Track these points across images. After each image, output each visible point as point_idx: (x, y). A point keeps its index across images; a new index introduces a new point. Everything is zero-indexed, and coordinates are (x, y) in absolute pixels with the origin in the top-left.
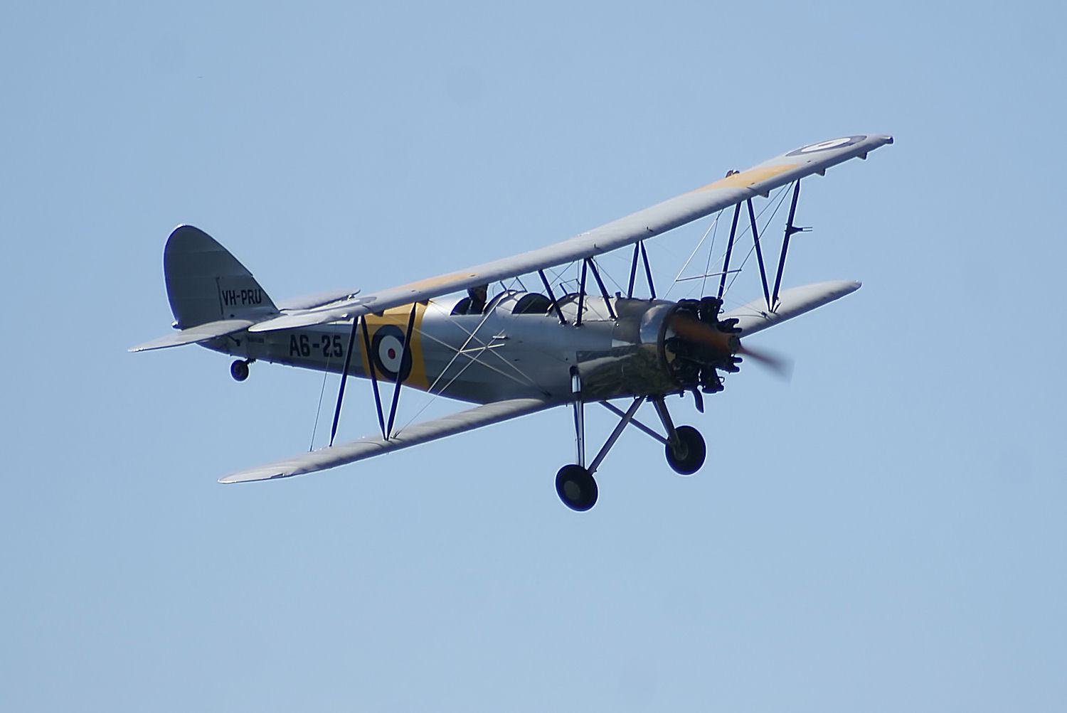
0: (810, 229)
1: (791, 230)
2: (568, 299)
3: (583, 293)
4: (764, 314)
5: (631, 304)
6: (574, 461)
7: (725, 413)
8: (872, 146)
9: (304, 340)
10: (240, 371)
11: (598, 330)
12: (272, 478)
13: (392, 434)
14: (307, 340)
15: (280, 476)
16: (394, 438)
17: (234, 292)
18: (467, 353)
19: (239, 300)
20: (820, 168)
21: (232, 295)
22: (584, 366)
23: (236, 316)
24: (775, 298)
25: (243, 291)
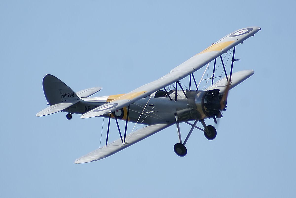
1: (233, 60)
2: (171, 92)
3: (176, 90)
5: (192, 93)
6: (179, 142)
7: (223, 124)
8: (255, 32)
9: (89, 107)
10: (69, 117)
11: (182, 101)
13: (125, 142)
14: (90, 107)
15: (94, 160)
17: (65, 93)
20: (241, 41)
22: (179, 112)
23: (67, 101)
24: (230, 80)
25: (68, 93)
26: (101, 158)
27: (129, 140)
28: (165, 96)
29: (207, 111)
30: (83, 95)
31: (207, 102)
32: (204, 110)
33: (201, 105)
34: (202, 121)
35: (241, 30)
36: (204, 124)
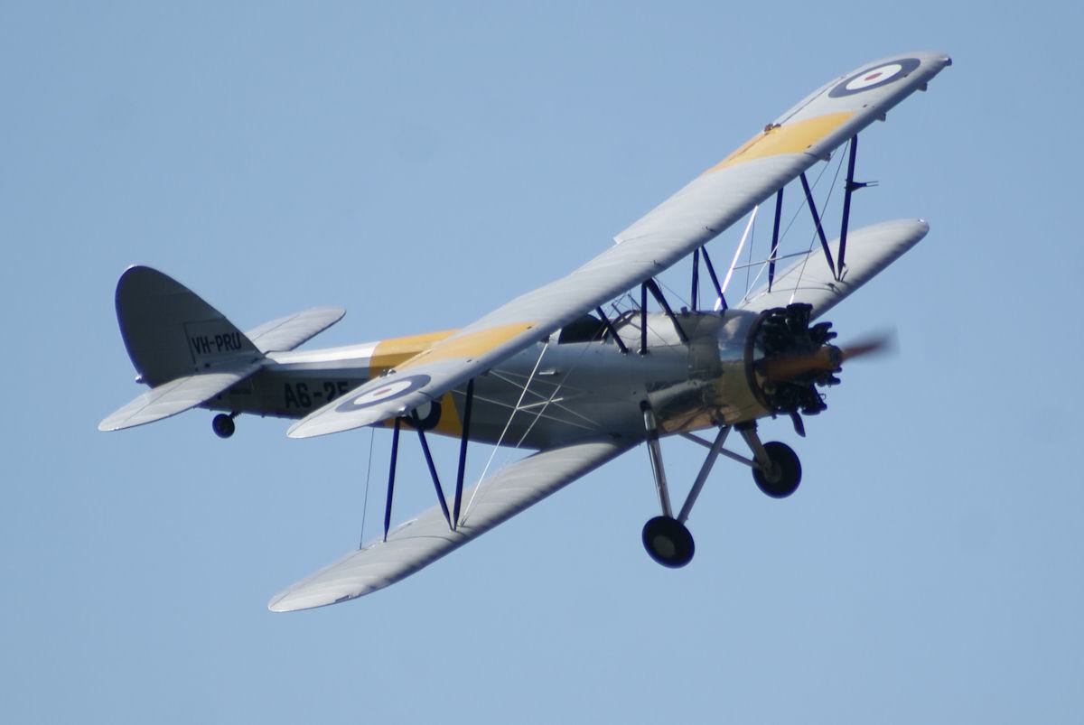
0: (876, 183)
1: (852, 186)
3: (643, 312)
4: (831, 285)
6: (658, 511)
8: (930, 74)
9: (302, 389)
10: (224, 427)
11: (666, 354)
12: (338, 601)
13: (459, 524)
14: (306, 389)
15: (346, 598)
16: (462, 525)
18: (530, 409)
19: (214, 348)
20: (879, 113)
21: (204, 342)
22: (656, 397)
23: (212, 365)
24: (841, 264)
25: (217, 337)
26: (373, 588)
27: (472, 512)
28: (599, 338)
29: (767, 391)
30: (275, 340)
31: (767, 353)
32: (753, 384)
33: (741, 366)
34: (748, 428)
35: (875, 68)
36: (752, 439)
